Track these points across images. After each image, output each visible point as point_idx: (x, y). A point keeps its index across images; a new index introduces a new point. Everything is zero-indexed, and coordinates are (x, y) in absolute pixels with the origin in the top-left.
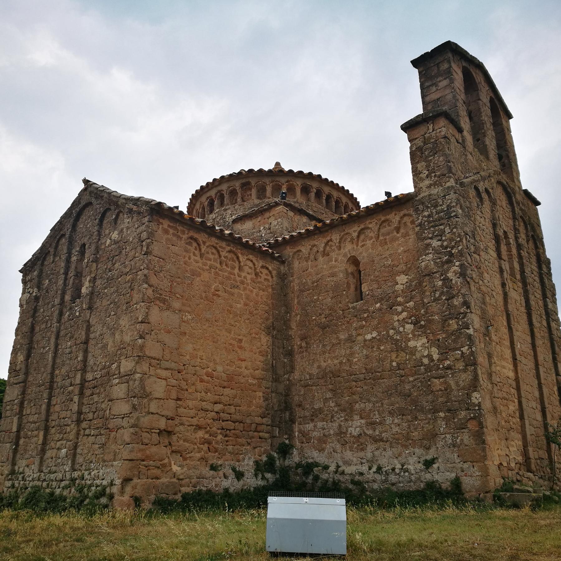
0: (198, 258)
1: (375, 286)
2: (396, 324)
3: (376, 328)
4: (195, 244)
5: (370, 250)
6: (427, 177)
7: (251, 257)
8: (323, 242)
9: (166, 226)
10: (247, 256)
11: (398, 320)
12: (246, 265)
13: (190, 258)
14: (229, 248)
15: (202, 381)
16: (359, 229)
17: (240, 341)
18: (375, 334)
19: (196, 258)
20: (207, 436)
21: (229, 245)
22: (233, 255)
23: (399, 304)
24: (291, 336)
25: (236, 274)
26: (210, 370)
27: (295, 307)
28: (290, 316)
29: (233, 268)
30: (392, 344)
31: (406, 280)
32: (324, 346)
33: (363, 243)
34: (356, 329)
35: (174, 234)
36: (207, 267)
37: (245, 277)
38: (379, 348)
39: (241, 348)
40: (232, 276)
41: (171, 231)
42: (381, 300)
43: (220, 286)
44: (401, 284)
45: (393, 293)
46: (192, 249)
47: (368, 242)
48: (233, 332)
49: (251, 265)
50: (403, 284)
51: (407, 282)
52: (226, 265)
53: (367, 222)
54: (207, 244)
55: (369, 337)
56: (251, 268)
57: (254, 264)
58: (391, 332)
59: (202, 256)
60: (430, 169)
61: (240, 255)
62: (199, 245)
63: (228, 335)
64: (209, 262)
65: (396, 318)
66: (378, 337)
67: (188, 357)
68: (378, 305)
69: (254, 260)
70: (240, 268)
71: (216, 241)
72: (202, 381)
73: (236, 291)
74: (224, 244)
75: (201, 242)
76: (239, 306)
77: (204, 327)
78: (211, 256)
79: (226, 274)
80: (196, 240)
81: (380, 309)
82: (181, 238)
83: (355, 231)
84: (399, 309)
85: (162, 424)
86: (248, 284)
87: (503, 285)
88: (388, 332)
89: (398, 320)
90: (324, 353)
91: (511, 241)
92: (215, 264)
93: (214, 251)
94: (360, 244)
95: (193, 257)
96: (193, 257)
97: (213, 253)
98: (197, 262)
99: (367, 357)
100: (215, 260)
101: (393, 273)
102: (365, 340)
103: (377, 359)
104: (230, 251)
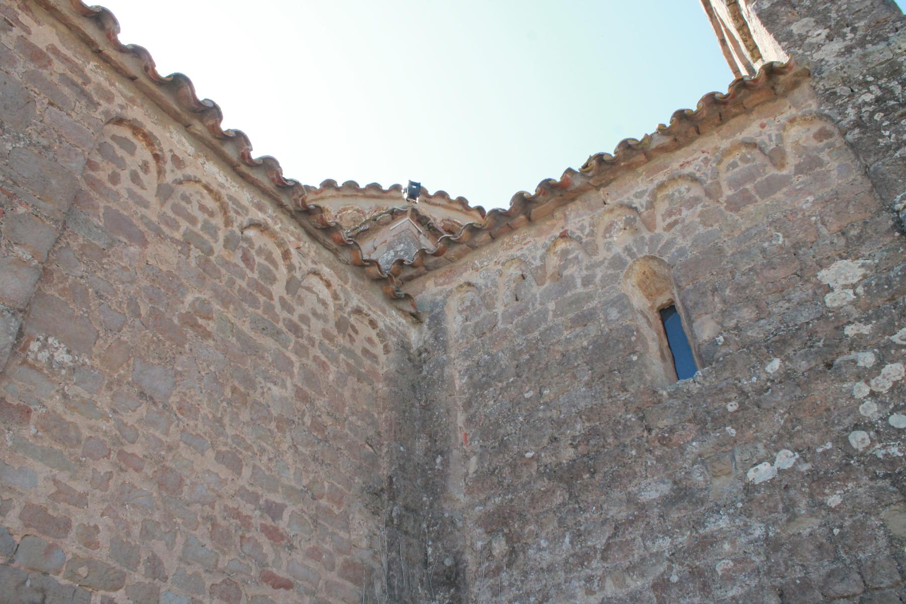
0: (149, 195)
1: (747, 314)
2: (870, 410)
3: (776, 444)
4: (143, 153)
5: (701, 229)
6: (829, 38)
7: (326, 271)
8: (539, 245)
10: (314, 262)
11: (873, 395)
16: (652, 187)
17: (274, 510)
18: (786, 459)
21: (260, 208)
23: (858, 344)
24: (453, 523)
25: (276, 298)
27: (460, 436)
28: (446, 463)
30: (874, 477)
31: (861, 271)
32: (578, 535)
33: (668, 221)
34: (700, 459)
36: (178, 235)
37: (304, 319)
38: (822, 504)
39: (274, 534)
41: (58, 67)
42: (777, 345)
44: (845, 287)
45: (822, 317)
47: (685, 212)
48: (246, 472)
49: (325, 294)
50: (854, 286)
51: (865, 276)
53: (675, 166)
55: (762, 473)
58: (859, 439)
60: (833, 23)
63: (224, 472)
64: (184, 225)
65: (862, 390)
66: (805, 467)
68: (775, 365)
69: (335, 281)
73: (268, 343)
75: (168, 156)
76: (276, 390)
77: (130, 419)
79: (244, 284)
80: (149, 140)
81: (787, 376)
83: (639, 195)
84: (867, 359)
86: (311, 341)
88: (842, 441)
89: (873, 395)
90: (583, 559)
94: (661, 224)
99: (772, 545)
101: (802, 262)
102: (749, 489)
103: (820, 547)
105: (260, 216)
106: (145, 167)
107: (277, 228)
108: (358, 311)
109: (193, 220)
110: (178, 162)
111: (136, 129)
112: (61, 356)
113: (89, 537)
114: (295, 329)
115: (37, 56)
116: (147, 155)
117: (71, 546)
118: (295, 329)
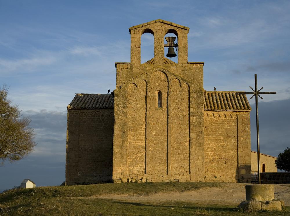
7: (106, 111)
9: (73, 112)
12: (105, 114)
13: (82, 118)
14: (96, 111)
15: (87, 152)
17: (102, 138)
19: (84, 118)
20: (90, 166)
22: (99, 112)
26: (90, 149)
29: (99, 116)
35: (76, 113)
36: (89, 119)
40: (99, 119)
41: (74, 113)
43: (94, 123)
46: (83, 115)
49: (107, 113)
52: (96, 116)
54: (88, 112)
56: (107, 114)
57: (108, 113)
59: (86, 116)
61: (101, 112)
62: (85, 113)
64: (89, 117)
67: (83, 146)
69: (107, 111)
70: (102, 116)
71: (91, 110)
72: (87, 152)
74: (94, 110)
76: (101, 128)
78: (90, 115)
80: (84, 112)
82: (78, 114)
85: (74, 164)
86: (105, 120)
87: (146, 114)
91: (163, 92)
92: (92, 117)
93: (91, 113)
95: (83, 117)
96: (83, 117)
97: (91, 114)
98: (85, 118)
100: (92, 116)
104: (97, 112)
105: (96, 111)
106: (84, 115)
107: (99, 111)
108: (111, 112)
109: (90, 116)
110: (86, 112)
111: (82, 112)
112: (83, 135)
113: (87, 146)
114: (103, 120)
115: (73, 113)
116: (84, 113)
117: (86, 147)
118: (103, 120)
